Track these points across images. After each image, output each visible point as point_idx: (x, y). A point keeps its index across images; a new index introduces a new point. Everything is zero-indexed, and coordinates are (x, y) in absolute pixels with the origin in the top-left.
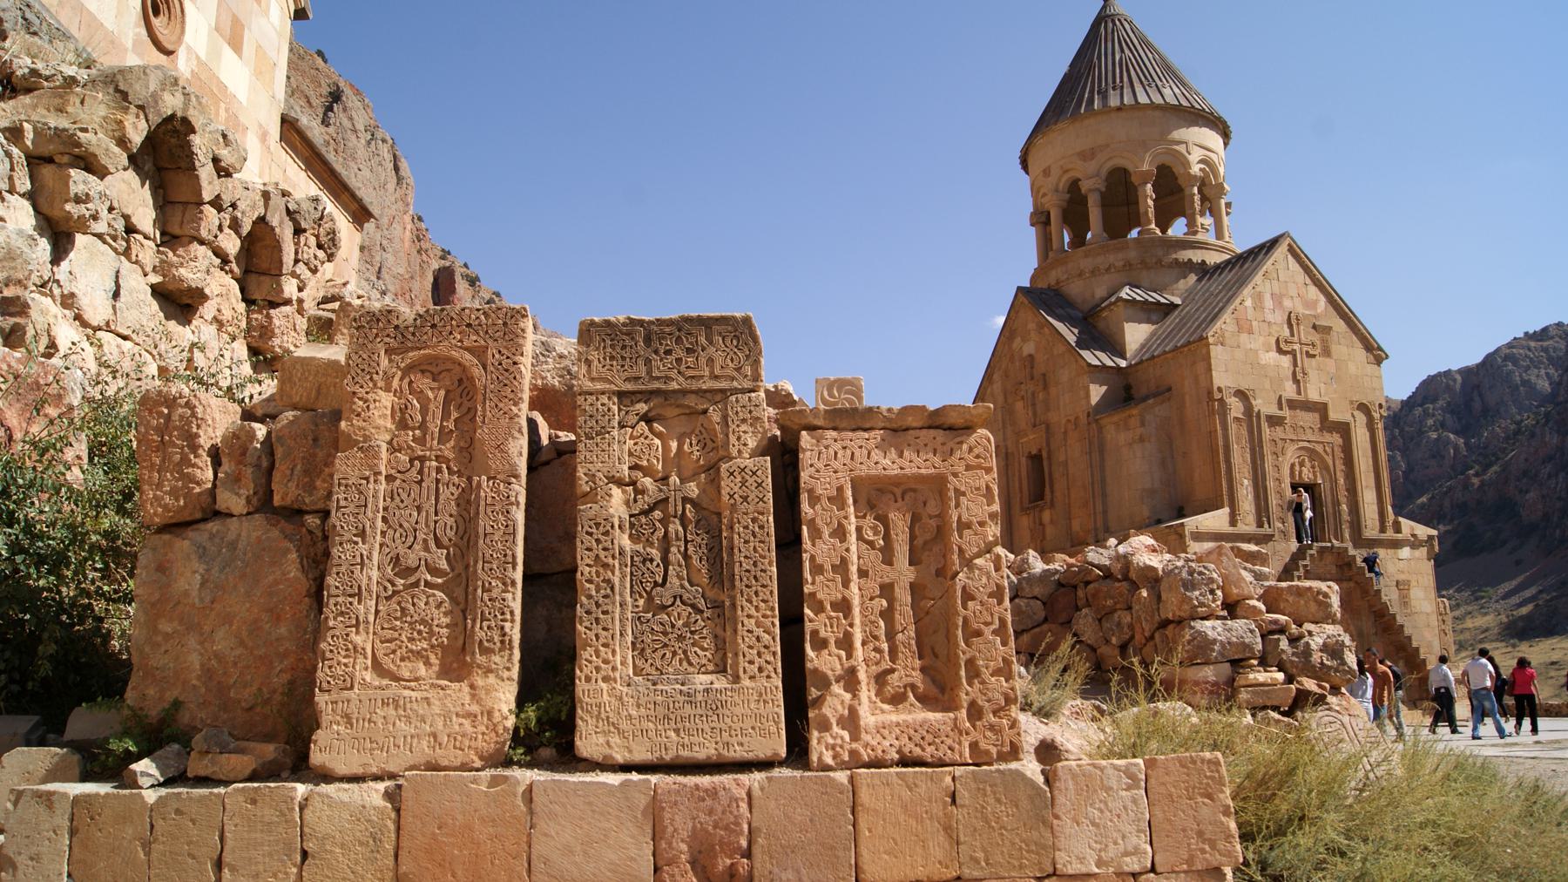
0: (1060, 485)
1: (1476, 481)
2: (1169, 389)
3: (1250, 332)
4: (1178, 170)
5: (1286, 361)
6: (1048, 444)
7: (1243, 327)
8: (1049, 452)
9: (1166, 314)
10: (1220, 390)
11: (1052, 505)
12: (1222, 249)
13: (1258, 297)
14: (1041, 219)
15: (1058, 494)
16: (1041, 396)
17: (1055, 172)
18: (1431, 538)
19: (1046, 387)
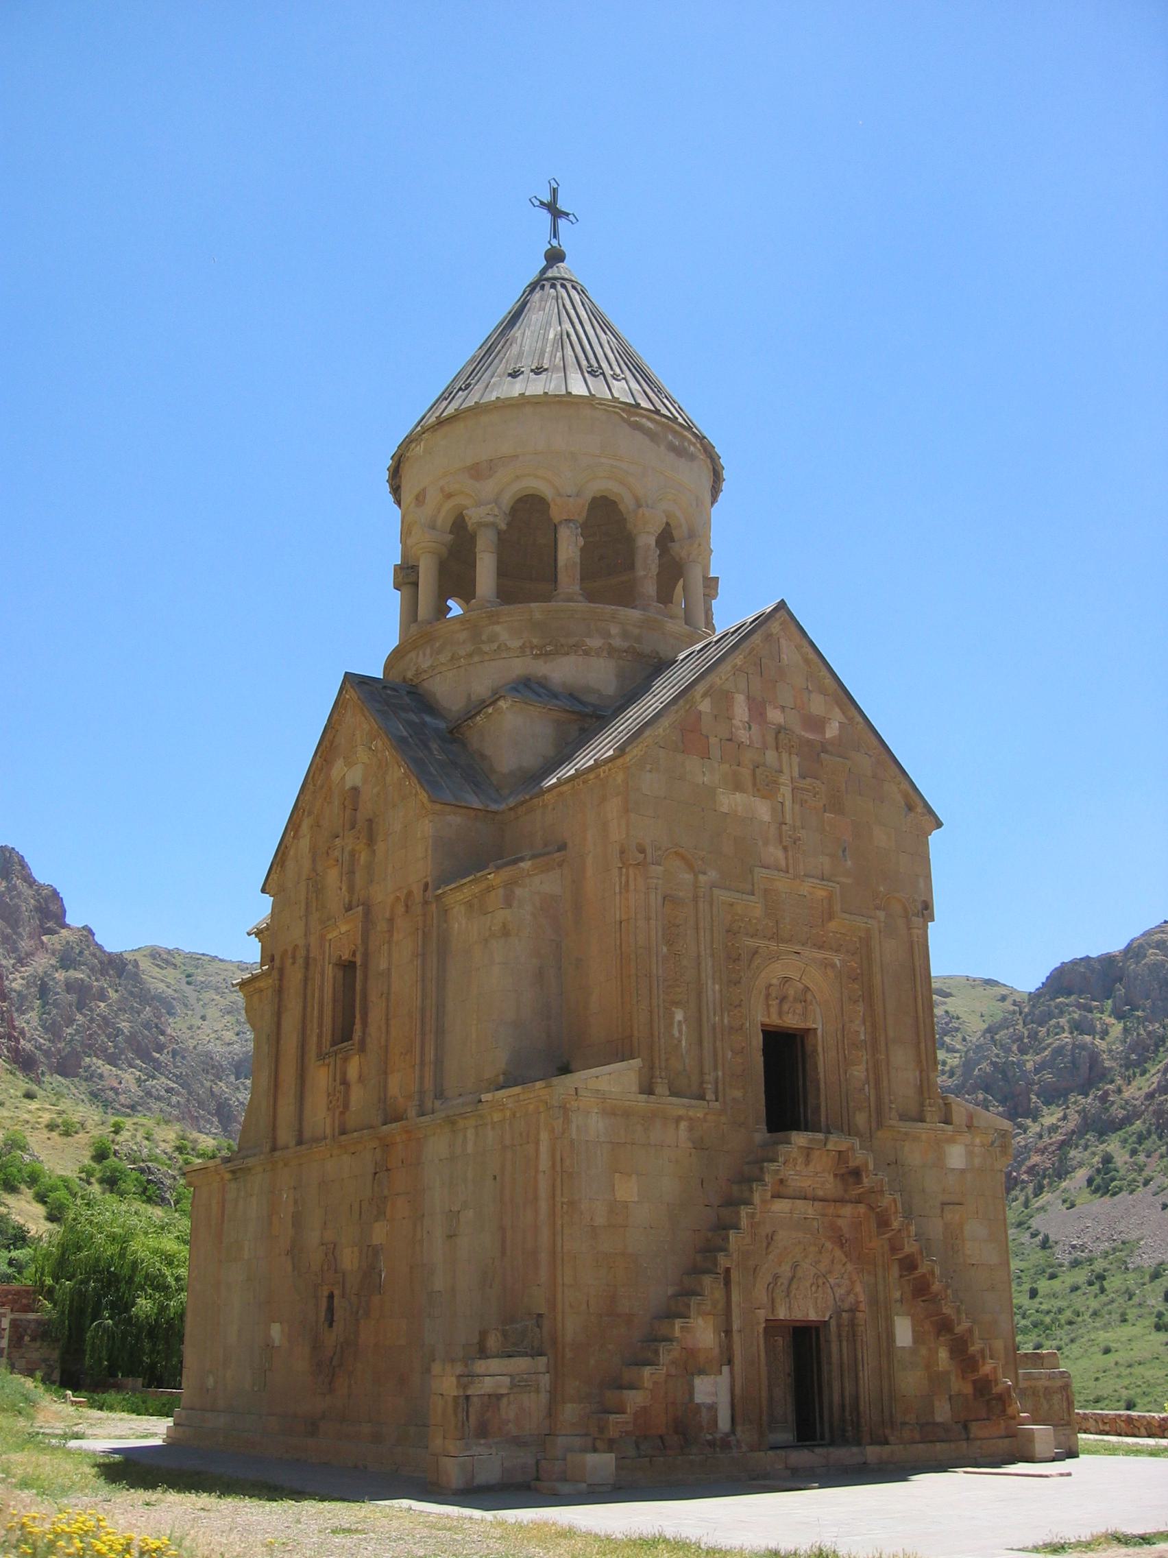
0: (376, 1015)
2: (562, 847)
3: (706, 755)
5: (763, 811)
6: (365, 941)
8: (366, 955)
11: (362, 1048)
14: (406, 576)
15: (372, 1029)
16: (363, 858)
19: (371, 841)
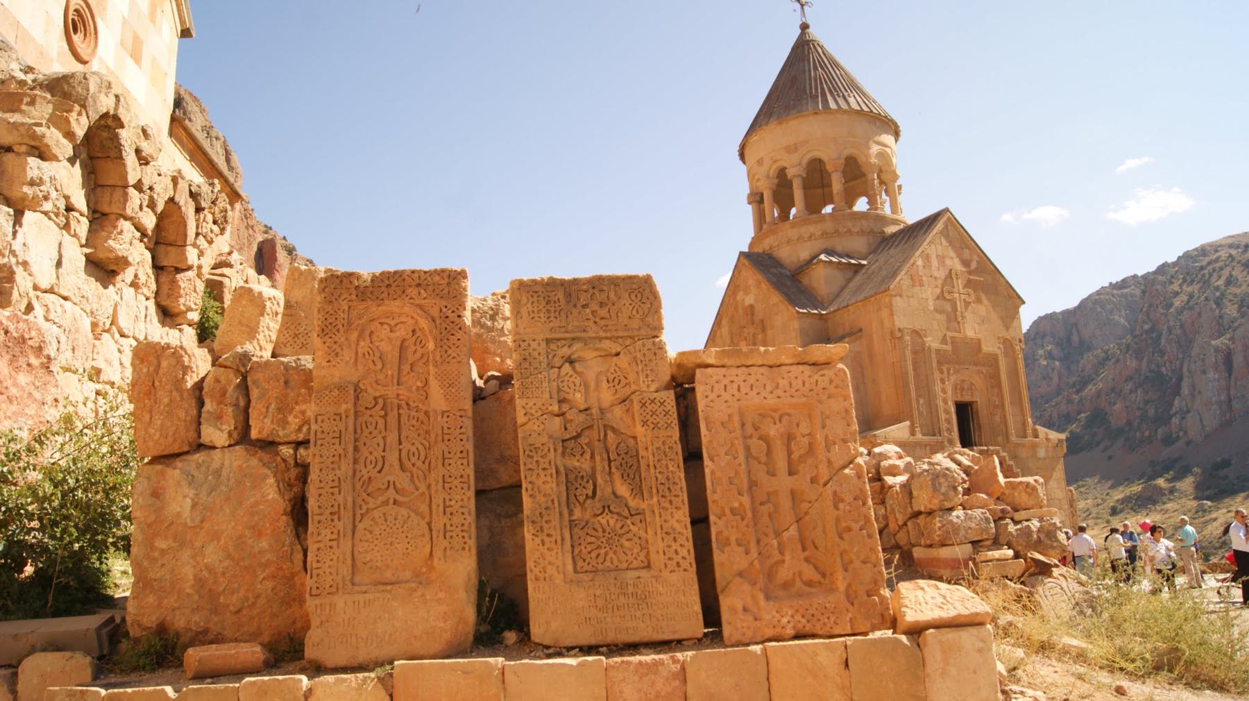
1: (1076, 397)
2: (861, 330)
3: (921, 285)
4: (861, 159)
7: (916, 281)
9: (856, 272)
10: (900, 330)
12: (896, 222)
13: (927, 258)
14: (756, 199)
16: (760, 337)
17: (767, 163)
18: (1060, 441)
19: (764, 330)
